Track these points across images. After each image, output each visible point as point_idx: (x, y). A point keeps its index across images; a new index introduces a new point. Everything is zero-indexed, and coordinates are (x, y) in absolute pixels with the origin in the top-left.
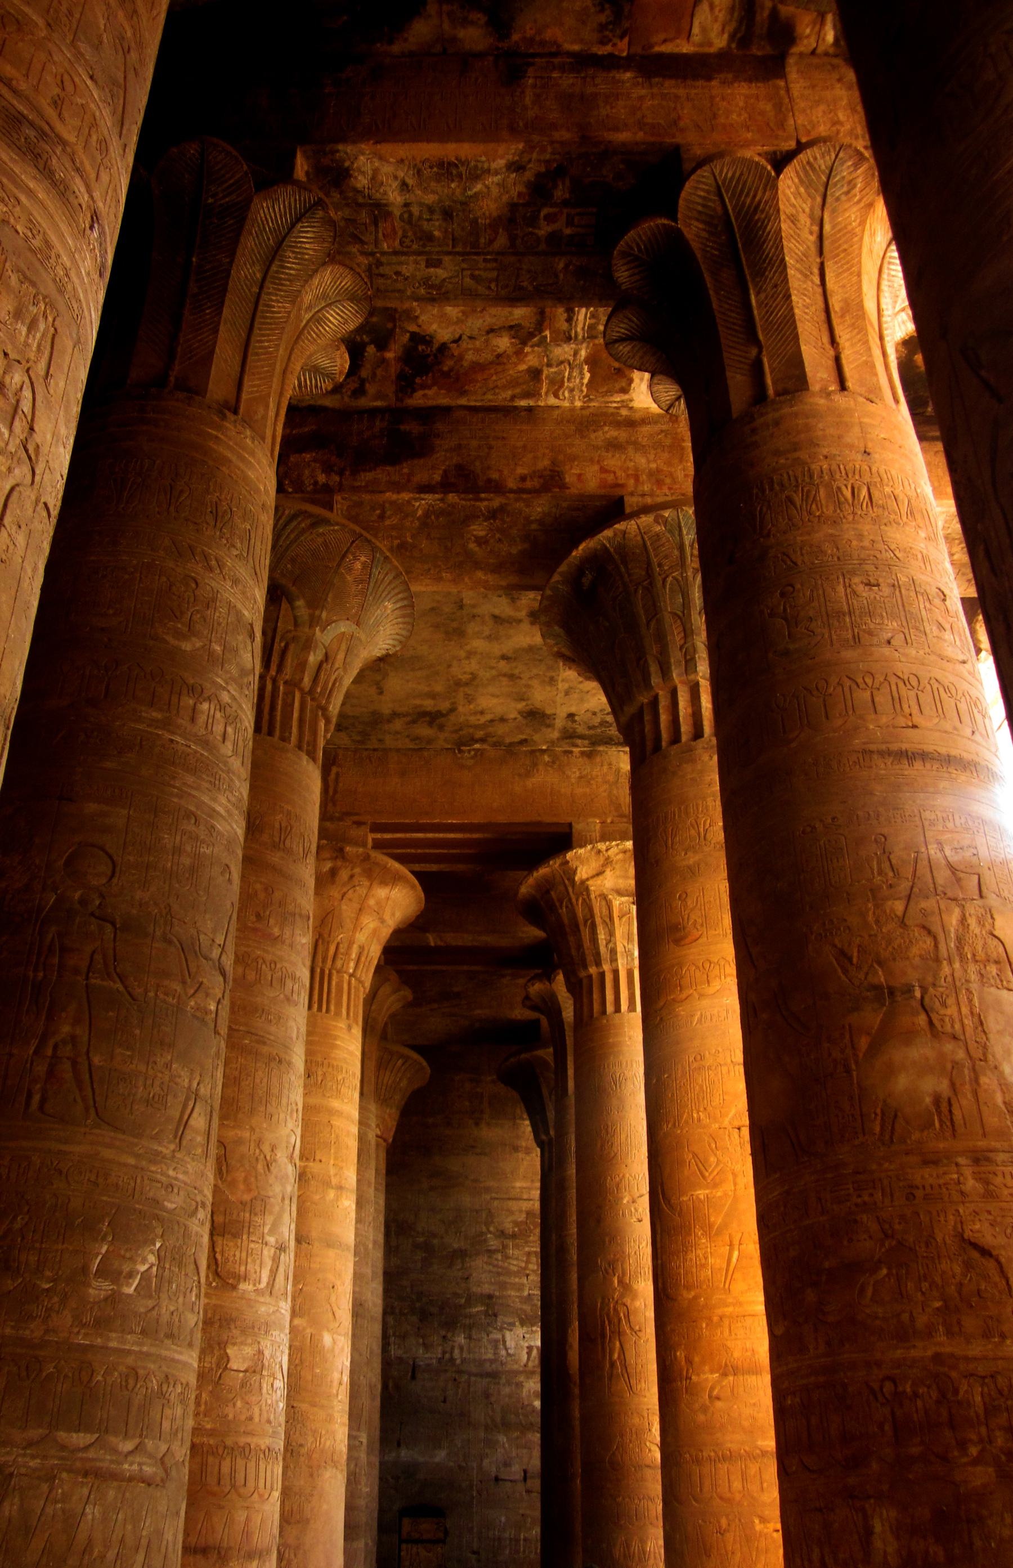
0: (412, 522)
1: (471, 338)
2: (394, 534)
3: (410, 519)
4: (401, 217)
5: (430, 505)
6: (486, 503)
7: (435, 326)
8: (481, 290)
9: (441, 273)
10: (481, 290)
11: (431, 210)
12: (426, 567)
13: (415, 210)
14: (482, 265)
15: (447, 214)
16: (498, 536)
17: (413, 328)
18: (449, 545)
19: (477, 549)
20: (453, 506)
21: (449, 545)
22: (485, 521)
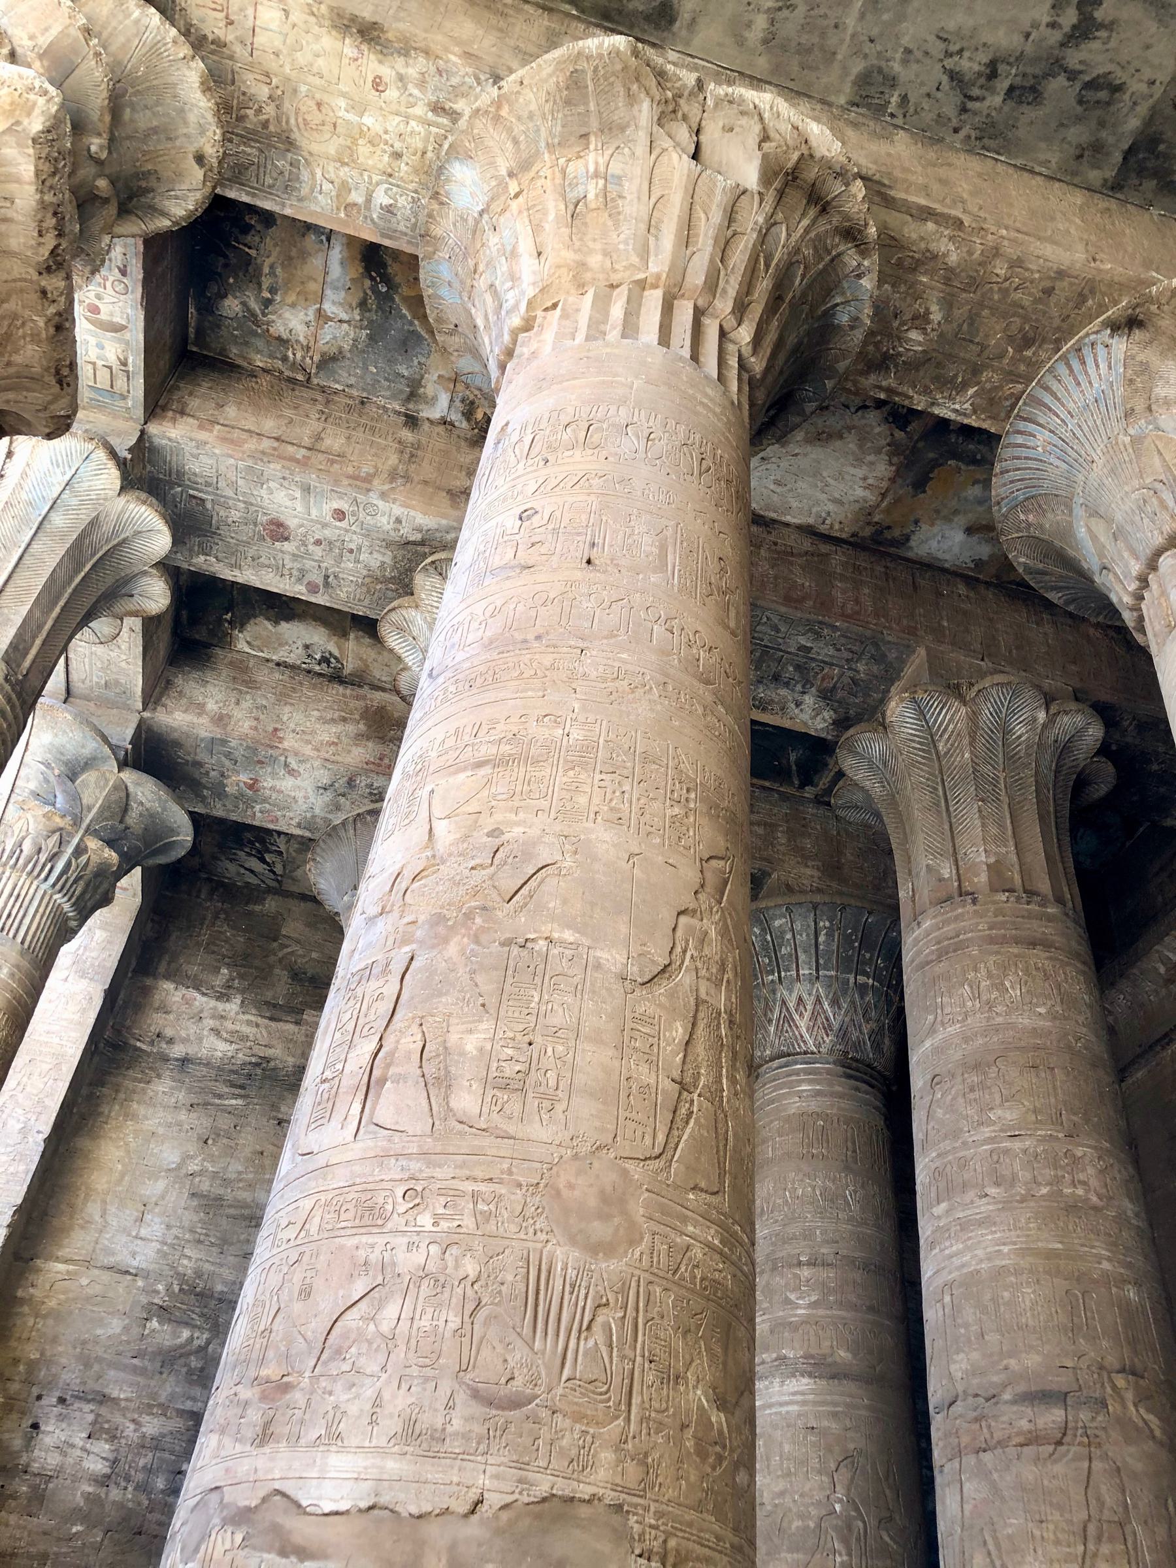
0: (989, 380)
1: (847, 407)
2: (1023, 367)
3: (988, 386)
4: (812, 685)
5: (950, 398)
6: (884, 383)
7: (877, 430)
8: (775, 619)
9: (803, 641)
10: (775, 619)
11: (787, 685)
12: (1018, 296)
13: (799, 688)
14: (766, 638)
15: (776, 678)
16: (896, 324)
17: (899, 434)
18: (965, 326)
19: (934, 308)
20: (926, 391)
21: (965, 326)
22: (900, 354)
